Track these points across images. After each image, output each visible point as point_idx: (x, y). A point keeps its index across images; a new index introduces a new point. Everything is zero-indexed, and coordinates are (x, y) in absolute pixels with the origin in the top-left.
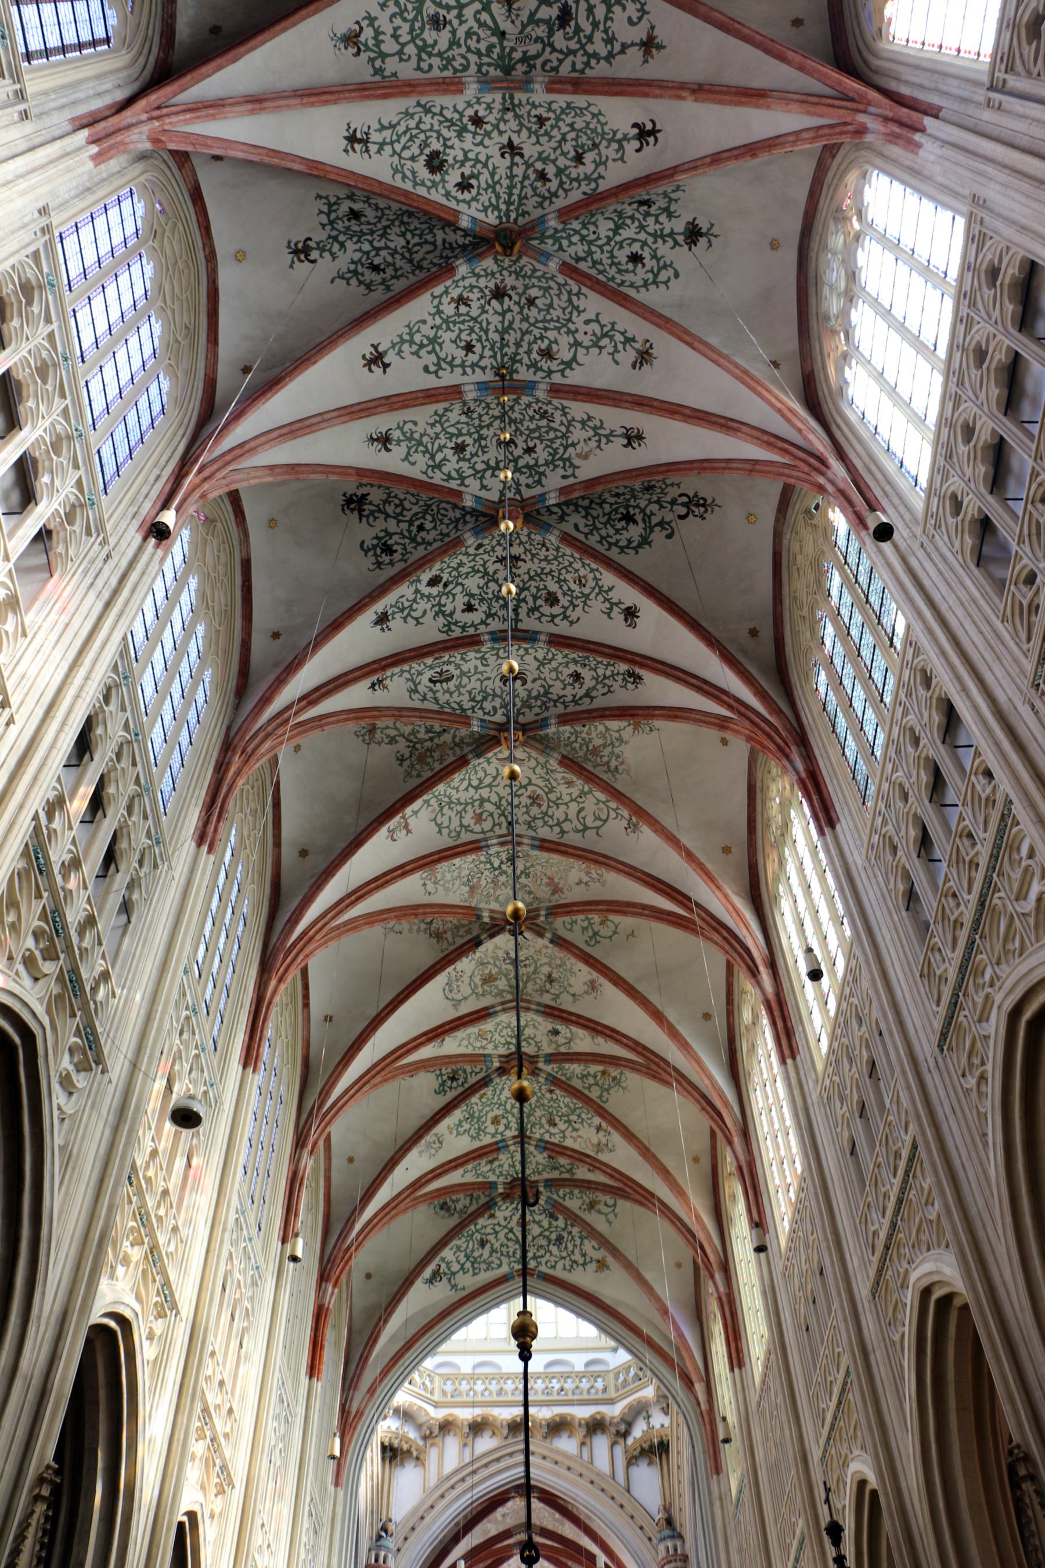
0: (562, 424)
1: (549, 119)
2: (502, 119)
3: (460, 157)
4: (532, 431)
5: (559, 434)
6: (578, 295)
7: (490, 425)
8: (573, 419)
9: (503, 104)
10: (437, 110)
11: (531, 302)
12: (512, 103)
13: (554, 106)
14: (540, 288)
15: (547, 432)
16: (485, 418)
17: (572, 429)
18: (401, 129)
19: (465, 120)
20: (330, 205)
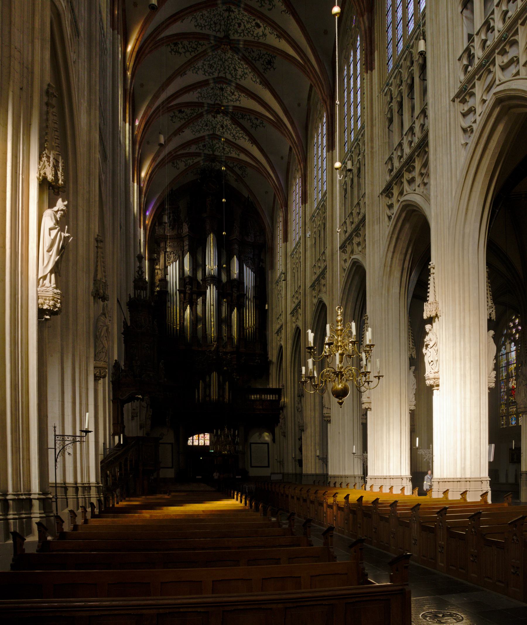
0: (205, 65)
1: (205, 126)
2: (216, 125)
3: (227, 121)
4: (214, 58)
5: (207, 60)
6: (199, 97)
7: (229, 58)
8: (201, 69)
9: (215, 130)
10: (232, 135)
11: (212, 89)
12: (213, 129)
13: (203, 131)
14: (209, 93)
15: (210, 58)
16: (230, 62)
17: (202, 64)
18: (241, 135)
19: (225, 128)
20: (262, 123)
